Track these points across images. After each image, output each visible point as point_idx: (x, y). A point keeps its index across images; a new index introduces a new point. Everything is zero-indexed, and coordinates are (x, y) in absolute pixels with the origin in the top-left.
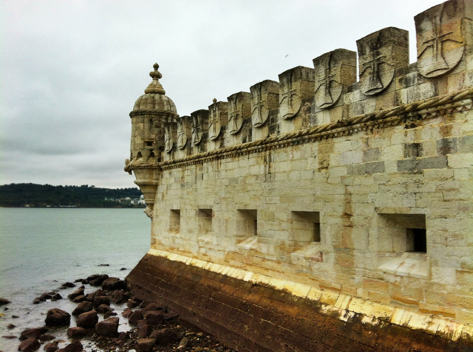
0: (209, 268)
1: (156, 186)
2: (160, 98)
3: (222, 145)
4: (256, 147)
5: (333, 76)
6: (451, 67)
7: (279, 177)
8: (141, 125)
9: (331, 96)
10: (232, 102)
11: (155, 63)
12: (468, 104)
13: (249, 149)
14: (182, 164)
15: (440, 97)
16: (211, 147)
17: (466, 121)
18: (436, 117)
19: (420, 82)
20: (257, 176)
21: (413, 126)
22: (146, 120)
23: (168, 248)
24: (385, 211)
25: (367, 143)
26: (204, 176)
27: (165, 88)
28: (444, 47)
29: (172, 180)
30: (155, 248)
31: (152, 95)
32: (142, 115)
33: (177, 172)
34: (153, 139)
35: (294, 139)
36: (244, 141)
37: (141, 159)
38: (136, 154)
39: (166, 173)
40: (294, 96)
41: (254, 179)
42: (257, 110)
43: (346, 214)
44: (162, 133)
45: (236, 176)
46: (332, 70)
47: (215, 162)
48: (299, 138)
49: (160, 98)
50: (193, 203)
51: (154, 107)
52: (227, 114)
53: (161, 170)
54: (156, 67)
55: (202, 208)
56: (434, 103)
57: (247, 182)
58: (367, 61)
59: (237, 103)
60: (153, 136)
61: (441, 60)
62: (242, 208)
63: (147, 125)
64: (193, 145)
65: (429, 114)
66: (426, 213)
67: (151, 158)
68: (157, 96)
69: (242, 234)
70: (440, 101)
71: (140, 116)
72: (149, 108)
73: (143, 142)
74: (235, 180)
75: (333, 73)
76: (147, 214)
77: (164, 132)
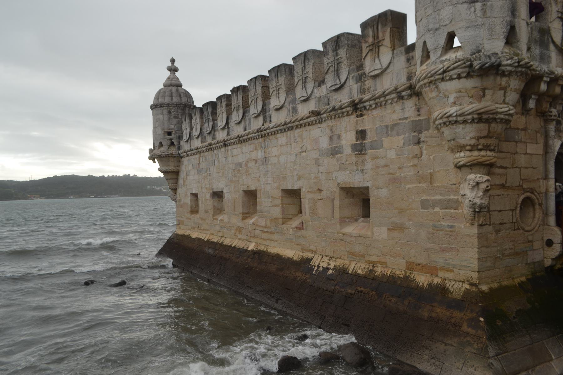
0: (222, 242)
1: (177, 173)
2: (177, 90)
3: (228, 134)
4: (254, 135)
5: (307, 73)
6: (384, 67)
7: (274, 160)
8: (161, 116)
9: (306, 89)
10: (234, 94)
11: (171, 58)
12: (395, 98)
13: (249, 136)
14: (199, 151)
15: (376, 92)
16: (221, 135)
17: (394, 112)
18: (375, 108)
19: (366, 79)
20: (256, 161)
21: (362, 115)
22: (165, 111)
23: (190, 228)
24: (344, 186)
25: (331, 130)
26: (216, 162)
27: (182, 81)
28: (380, 52)
29: (190, 167)
30: (180, 228)
31: (170, 88)
32: (161, 107)
33: (194, 159)
34: (172, 129)
35: (282, 127)
36: (245, 130)
37: (162, 149)
38: (157, 144)
39: (185, 161)
40: (280, 89)
41: (253, 163)
42: (253, 101)
43: (319, 189)
44: (180, 123)
45: (240, 161)
46: (307, 67)
47: (223, 149)
48: (285, 126)
49: (177, 90)
50: (208, 186)
51: (172, 99)
52: (231, 105)
53: (181, 157)
54: (173, 61)
55: (215, 190)
56: (373, 97)
57: (248, 166)
58: (330, 61)
59: (239, 96)
60: (172, 127)
61: (377, 60)
62: (246, 188)
63: (166, 117)
64: (205, 134)
65: (371, 106)
66: (369, 185)
67: (172, 147)
68: (174, 89)
69: (247, 212)
70: (377, 95)
71: (159, 109)
72: (167, 100)
73: (163, 132)
74: (240, 164)
75: (307, 71)
76: (172, 199)
77: (182, 122)
